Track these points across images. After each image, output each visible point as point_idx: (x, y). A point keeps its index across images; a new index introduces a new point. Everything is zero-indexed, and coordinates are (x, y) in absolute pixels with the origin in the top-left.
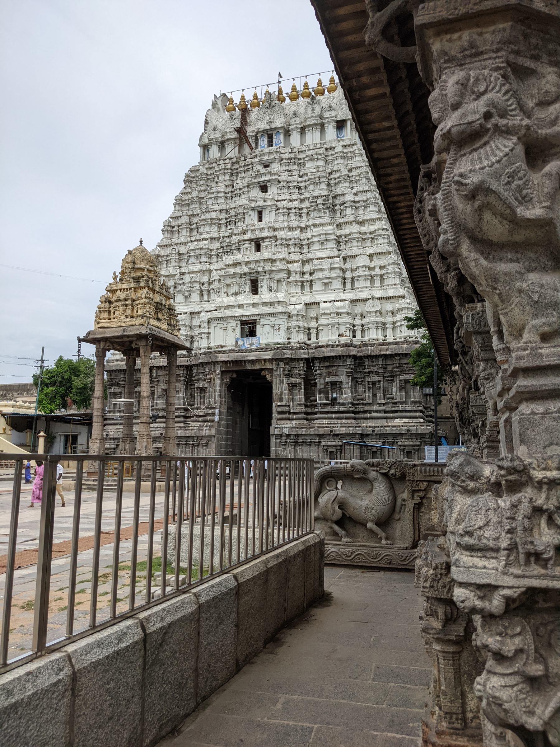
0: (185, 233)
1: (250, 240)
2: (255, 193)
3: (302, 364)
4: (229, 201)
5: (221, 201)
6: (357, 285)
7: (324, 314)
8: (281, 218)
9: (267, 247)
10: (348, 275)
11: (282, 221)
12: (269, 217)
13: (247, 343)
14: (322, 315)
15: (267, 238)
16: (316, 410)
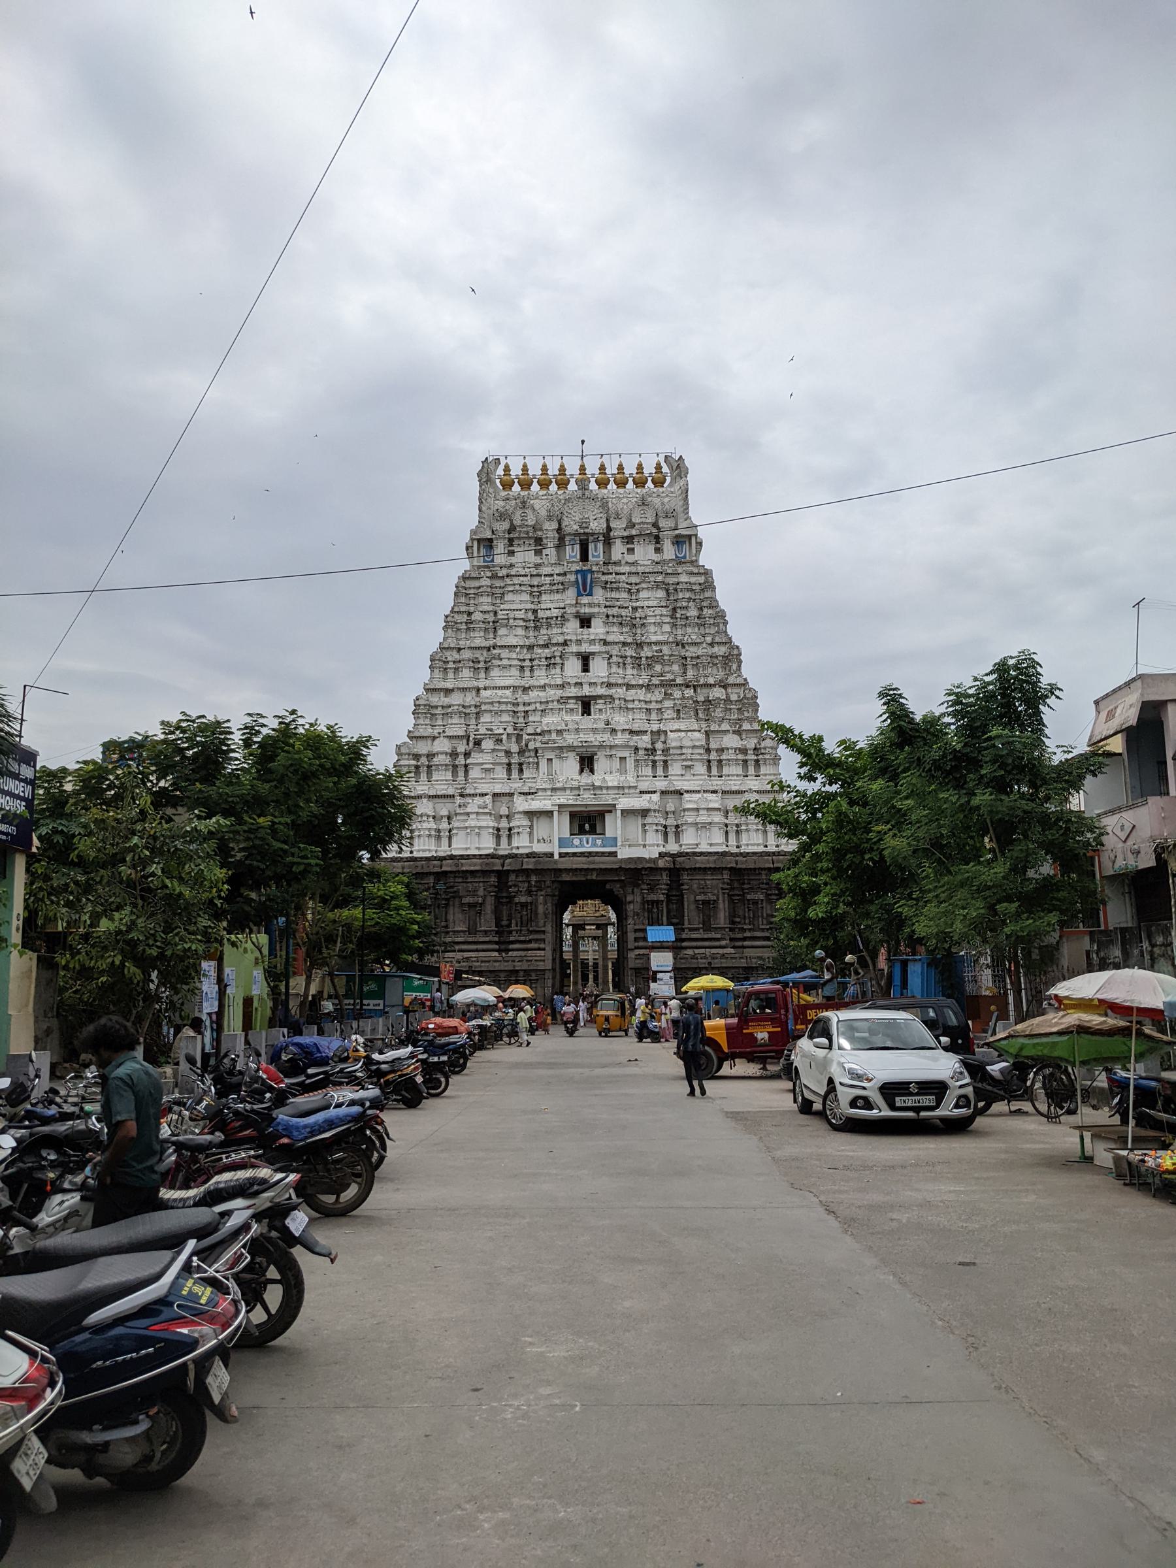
0: (466, 673)
1: (576, 698)
2: (573, 626)
3: (665, 878)
4: (531, 634)
5: (520, 632)
6: (726, 771)
7: (688, 810)
8: (614, 669)
9: (601, 710)
10: (714, 756)
11: (618, 675)
12: (599, 668)
13: (586, 844)
14: (684, 810)
15: (600, 697)
16: (684, 936)
